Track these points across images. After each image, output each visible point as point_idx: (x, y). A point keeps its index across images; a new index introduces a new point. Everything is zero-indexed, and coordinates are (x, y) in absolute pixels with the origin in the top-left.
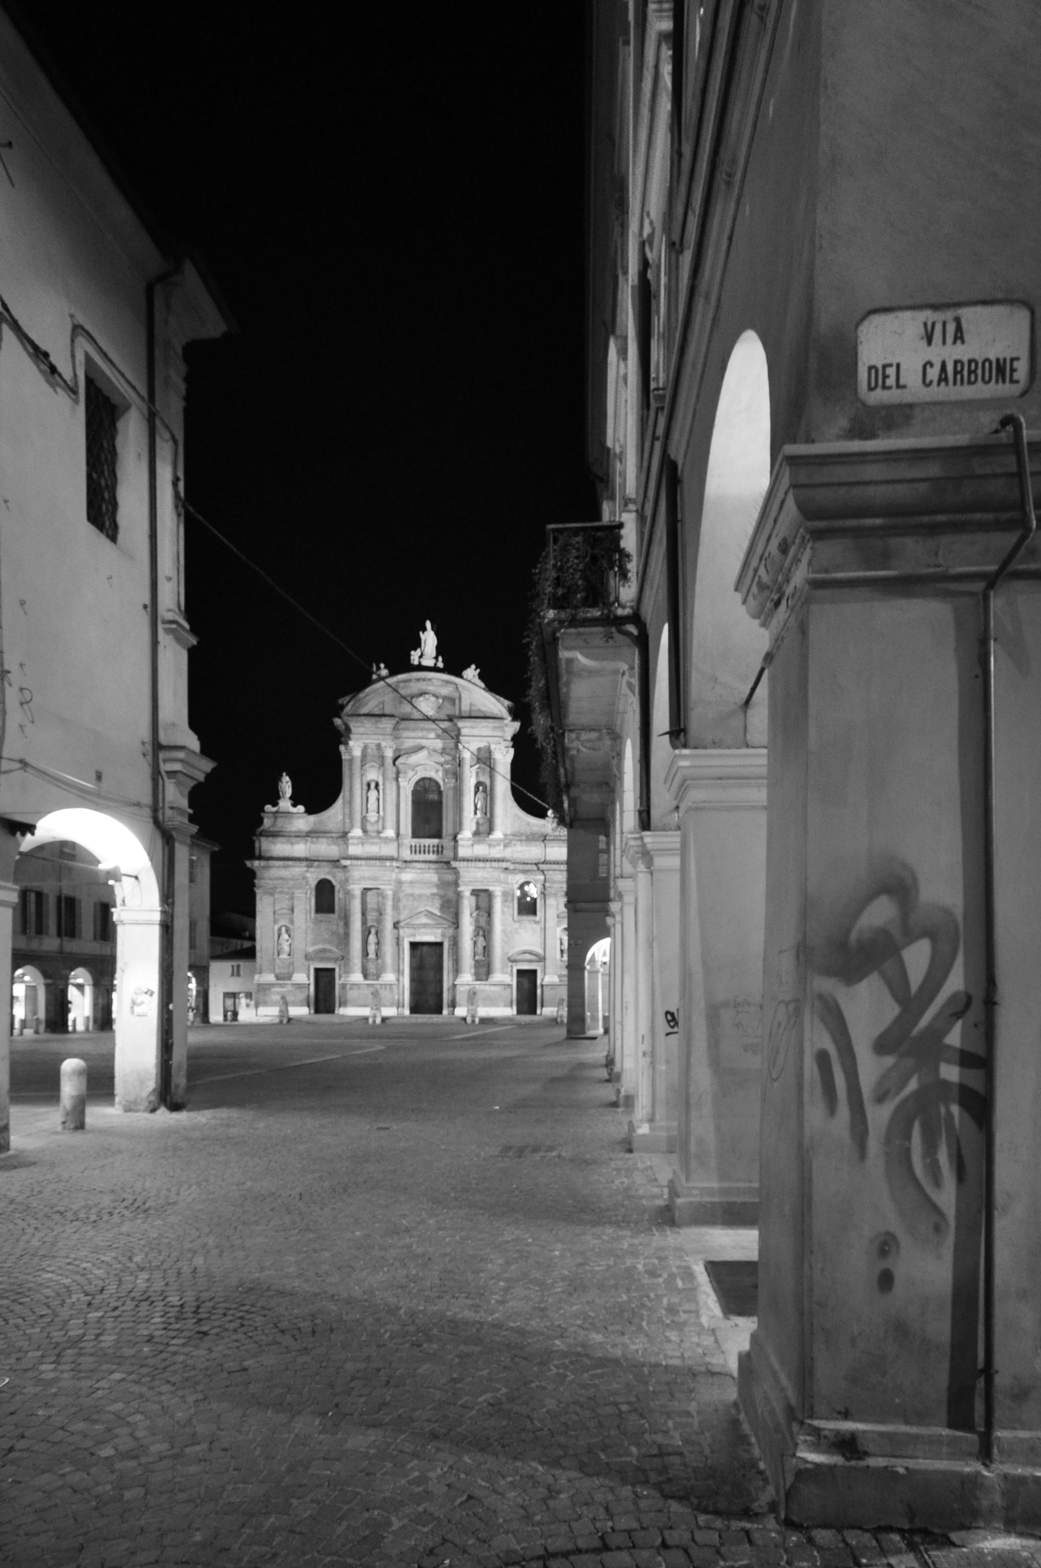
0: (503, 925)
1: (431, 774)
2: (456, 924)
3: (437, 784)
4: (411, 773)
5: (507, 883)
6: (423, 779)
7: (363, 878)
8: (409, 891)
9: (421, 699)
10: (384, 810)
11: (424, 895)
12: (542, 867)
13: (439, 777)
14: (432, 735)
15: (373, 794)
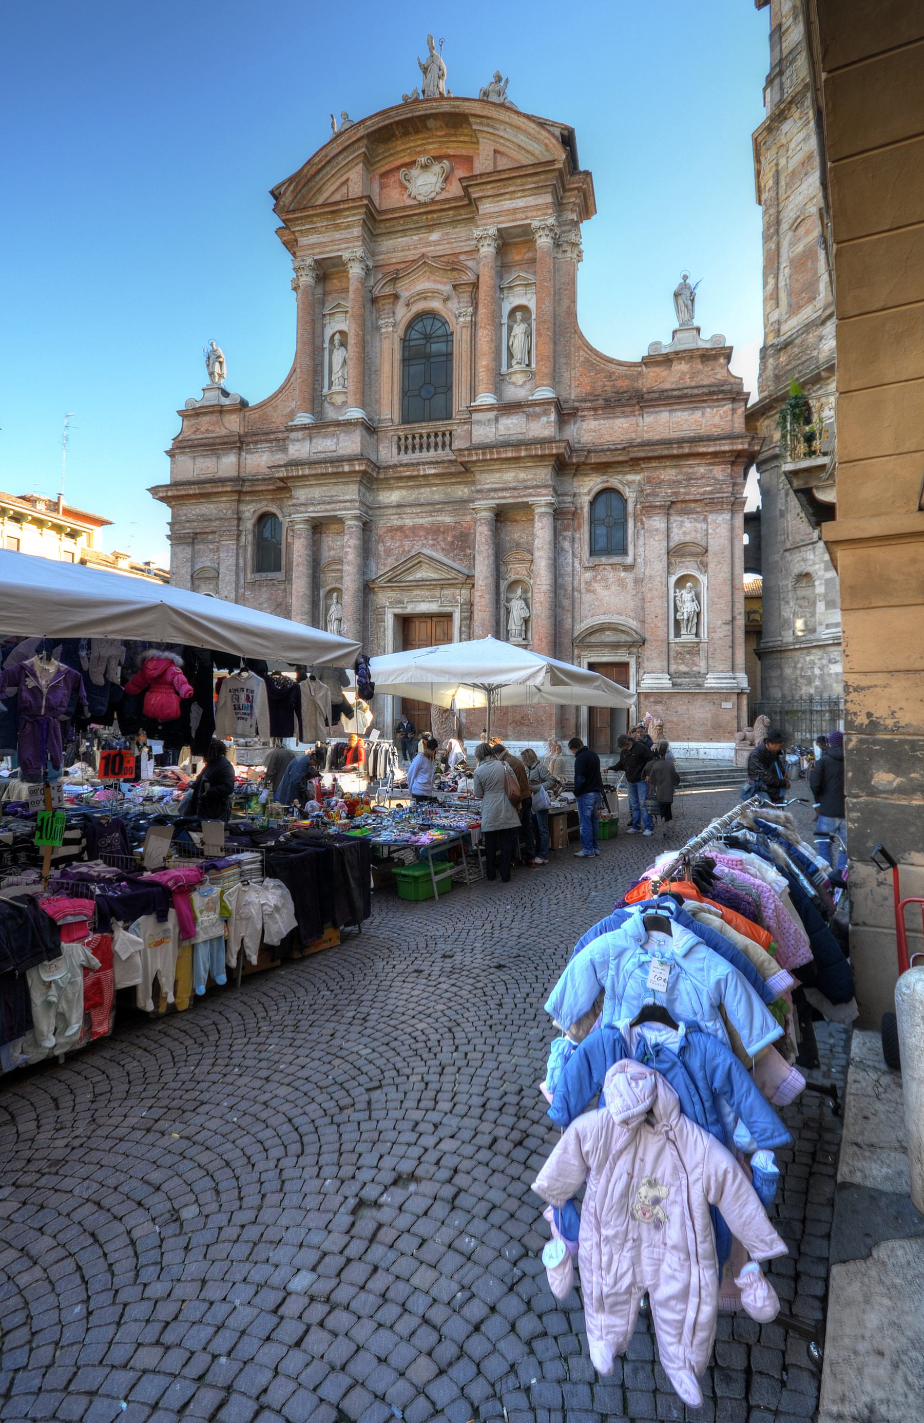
1: (435, 304)
6: (420, 316)
8: (396, 522)
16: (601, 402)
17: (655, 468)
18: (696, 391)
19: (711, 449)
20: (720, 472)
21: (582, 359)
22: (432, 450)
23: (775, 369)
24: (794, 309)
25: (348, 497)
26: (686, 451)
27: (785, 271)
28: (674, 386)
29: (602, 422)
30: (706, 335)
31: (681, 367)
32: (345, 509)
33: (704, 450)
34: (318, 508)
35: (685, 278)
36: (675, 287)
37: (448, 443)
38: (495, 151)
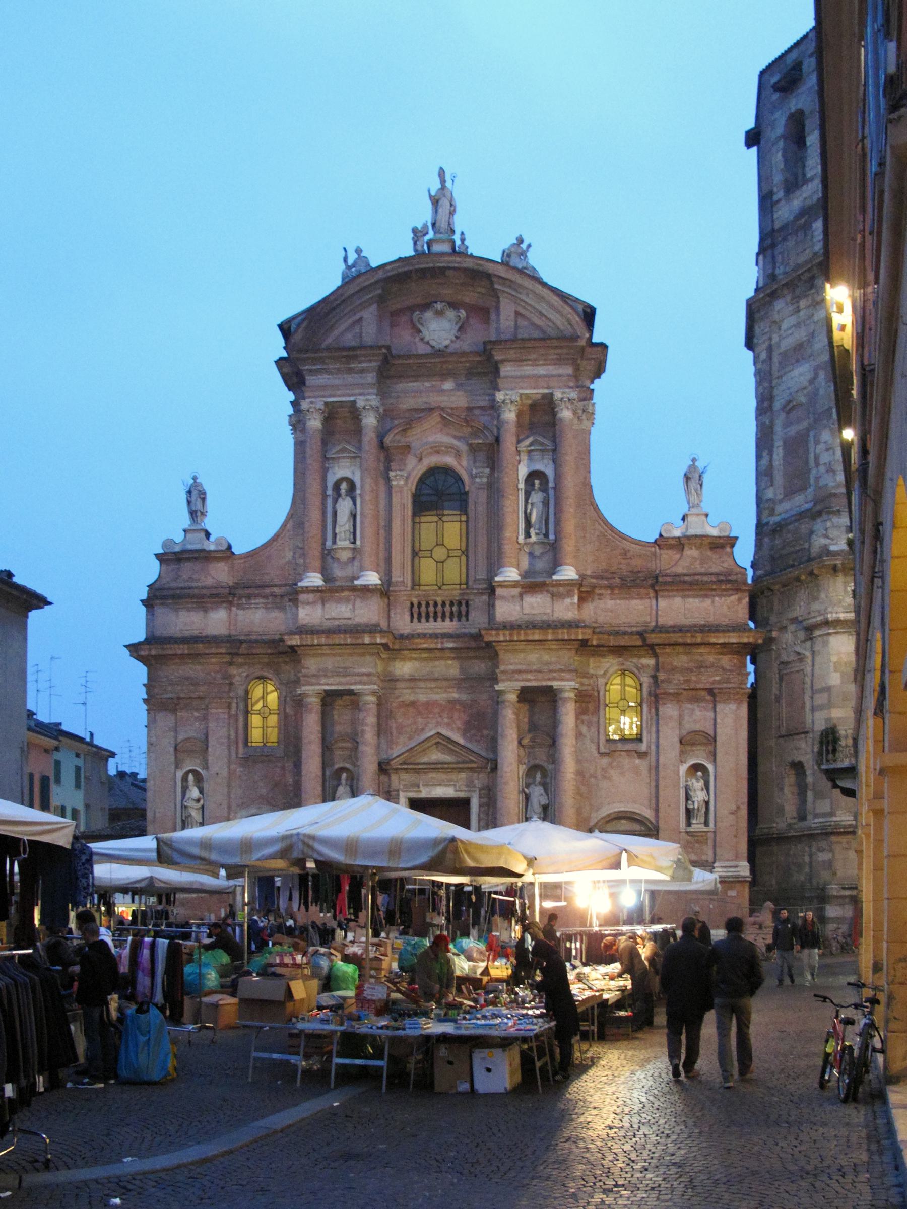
0: (578, 761)
1: (449, 460)
2: (493, 766)
3: (459, 479)
4: (411, 462)
5: (586, 675)
6: (432, 472)
7: (324, 673)
9: (429, 315)
10: (362, 538)
11: (435, 703)
12: (653, 638)
13: (462, 465)
14: (448, 385)
15: (344, 506)
16: (618, 581)
17: (669, 655)
18: (705, 579)
19: (721, 641)
20: (726, 661)
21: (597, 533)
22: (448, 619)
23: (771, 549)
24: (789, 493)
25: (363, 670)
26: (699, 640)
27: (779, 453)
28: (685, 571)
29: (618, 602)
30: (713, 520)
31: (691, 552)
32: (360, 683)
33: (713, 640)
34: (331, 680)
35: (694, 460)
36: (684, 469)
37: (464, 613)
38: (517, 314)
